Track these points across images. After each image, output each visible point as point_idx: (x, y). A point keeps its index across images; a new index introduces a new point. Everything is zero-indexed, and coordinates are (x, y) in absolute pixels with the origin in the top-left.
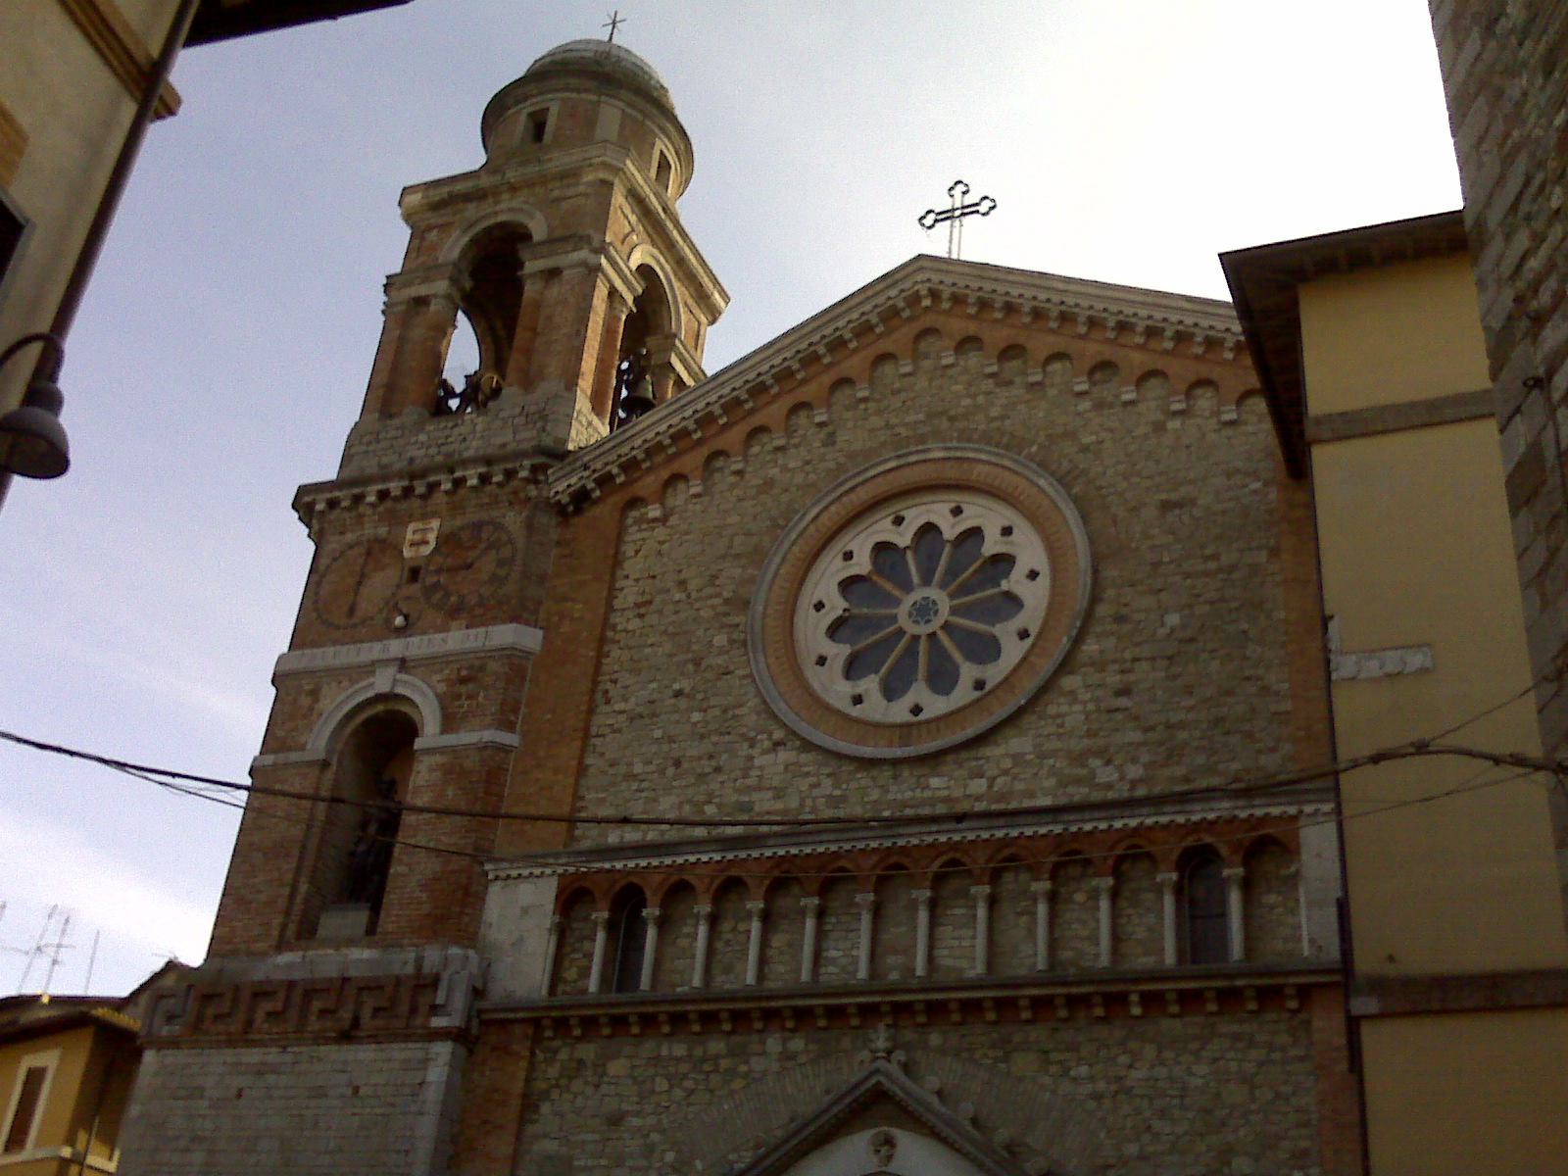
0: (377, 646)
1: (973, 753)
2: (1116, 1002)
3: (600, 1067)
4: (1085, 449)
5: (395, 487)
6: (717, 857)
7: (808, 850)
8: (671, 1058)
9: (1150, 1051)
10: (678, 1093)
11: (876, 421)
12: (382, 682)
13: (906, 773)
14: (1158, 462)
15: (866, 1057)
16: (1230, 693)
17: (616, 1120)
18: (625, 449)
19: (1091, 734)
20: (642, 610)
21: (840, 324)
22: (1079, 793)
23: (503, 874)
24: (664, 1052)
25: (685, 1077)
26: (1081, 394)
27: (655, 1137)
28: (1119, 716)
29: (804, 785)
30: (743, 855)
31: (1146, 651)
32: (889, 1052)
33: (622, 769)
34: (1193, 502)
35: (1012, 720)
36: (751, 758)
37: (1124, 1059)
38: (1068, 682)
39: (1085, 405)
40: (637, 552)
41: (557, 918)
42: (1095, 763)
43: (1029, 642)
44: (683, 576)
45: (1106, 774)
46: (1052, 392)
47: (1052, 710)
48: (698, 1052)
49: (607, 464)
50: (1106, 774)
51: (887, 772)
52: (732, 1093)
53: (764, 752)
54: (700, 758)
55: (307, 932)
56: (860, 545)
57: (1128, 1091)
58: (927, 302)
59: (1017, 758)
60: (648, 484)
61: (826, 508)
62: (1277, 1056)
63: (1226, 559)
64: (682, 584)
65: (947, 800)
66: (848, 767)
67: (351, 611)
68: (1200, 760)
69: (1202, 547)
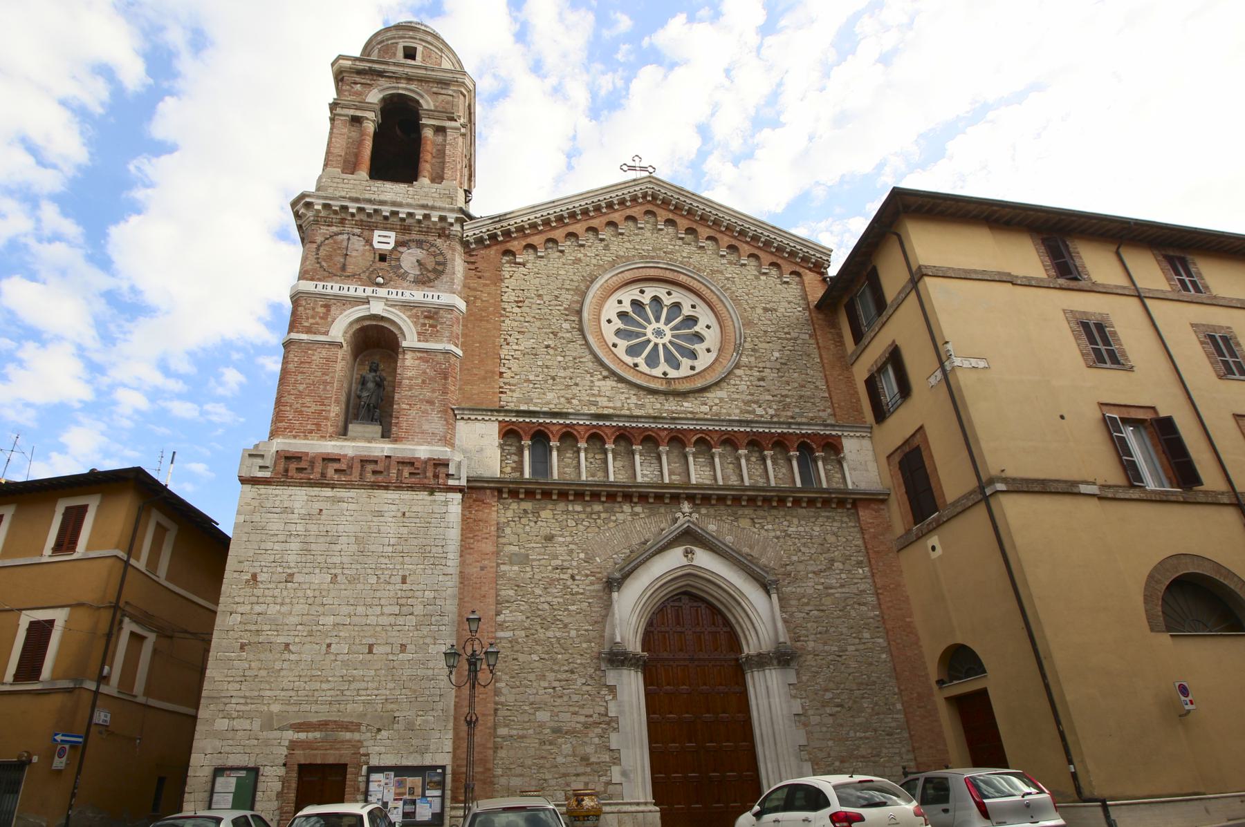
2: (782, 501)
3: (536, 513)
9: (795, 521)
11: (628, 245)
17: (550, 538)
22: (750, 417)
24: (570, 508)
35: (717, 384)
42: (755, 406)
48: (589, 509)
51: (661, 399)
59: (721, 399)
64: (540, 296)
65: (691, 413)
66: (642, 393)
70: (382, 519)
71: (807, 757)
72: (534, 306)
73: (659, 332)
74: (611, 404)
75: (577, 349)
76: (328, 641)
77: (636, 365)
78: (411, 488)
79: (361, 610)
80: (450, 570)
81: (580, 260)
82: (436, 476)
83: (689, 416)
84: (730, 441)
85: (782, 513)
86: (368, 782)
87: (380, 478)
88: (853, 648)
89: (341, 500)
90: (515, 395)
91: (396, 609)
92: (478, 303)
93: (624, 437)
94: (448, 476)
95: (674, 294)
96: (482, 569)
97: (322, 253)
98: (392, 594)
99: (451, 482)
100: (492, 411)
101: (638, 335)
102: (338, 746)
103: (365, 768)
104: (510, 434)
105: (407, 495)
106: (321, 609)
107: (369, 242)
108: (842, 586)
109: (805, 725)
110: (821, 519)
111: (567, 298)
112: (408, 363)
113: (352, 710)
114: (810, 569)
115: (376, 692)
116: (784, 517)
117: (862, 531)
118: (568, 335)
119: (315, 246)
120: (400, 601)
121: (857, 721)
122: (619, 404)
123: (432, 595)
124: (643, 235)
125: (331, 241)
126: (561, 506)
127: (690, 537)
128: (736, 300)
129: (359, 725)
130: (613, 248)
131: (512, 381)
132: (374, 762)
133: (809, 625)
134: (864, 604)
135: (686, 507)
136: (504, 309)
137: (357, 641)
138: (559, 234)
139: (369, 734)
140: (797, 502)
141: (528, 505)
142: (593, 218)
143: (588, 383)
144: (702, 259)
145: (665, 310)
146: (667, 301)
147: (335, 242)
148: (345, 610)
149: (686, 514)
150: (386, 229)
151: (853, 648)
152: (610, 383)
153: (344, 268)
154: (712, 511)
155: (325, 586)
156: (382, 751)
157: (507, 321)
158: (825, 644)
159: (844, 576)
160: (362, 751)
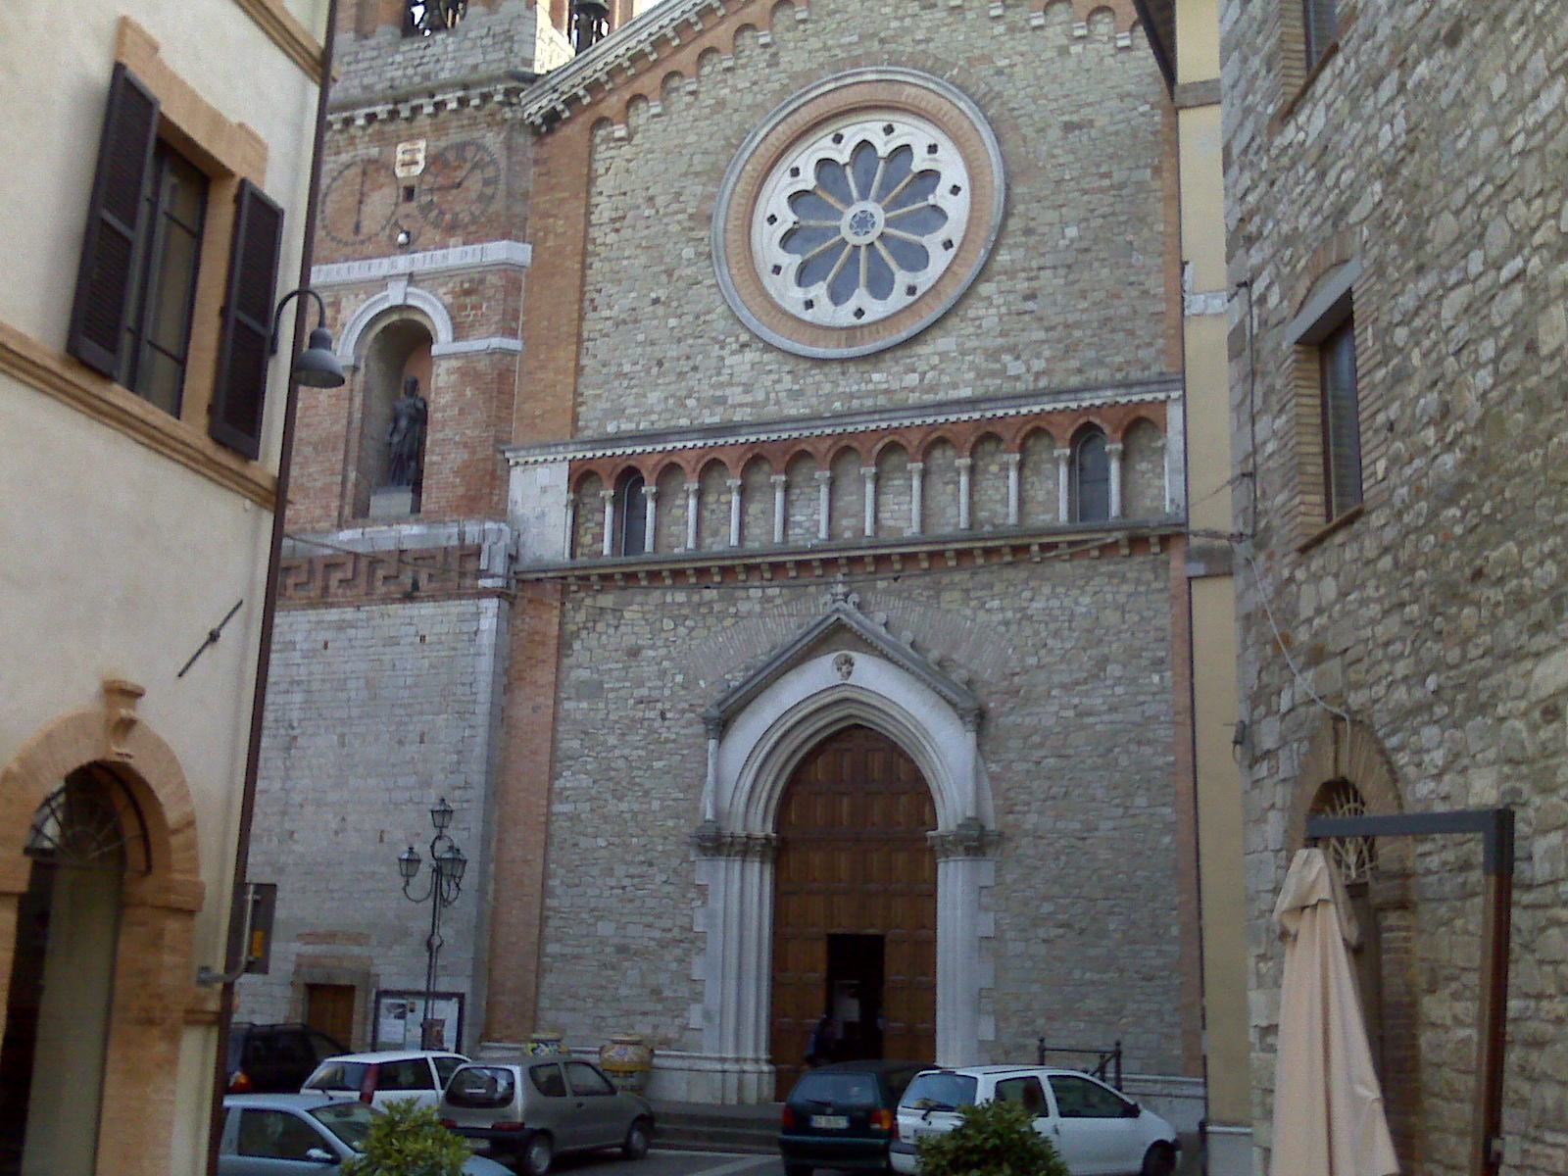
0: (386, 262)
1: (907, 352)
3: (617, 611)
4: (1000, 72)
5: (381, 110)
6: (700, 444)
7: (774, 437)
10: (682, 631)
12: (395, 295)
13: (852, 369)
14: (1062, 84)
15: (826, 601)
16: (1117, 296)
17: (634, 653)
18: (588, 72)
19: (1003, 334)
20: (617, 225)
22: (992, 384)
23: (522, 461)
24: (669, 599)
25: (686, 618)
27: (666, 664)
28: (1027, 318)
29: (768, 380)
30: (721, 442)
31: (1048, 260)
32: (846, 596)
33: (614, 369)
34: (1091, 123)
36: (722, 359)
38: (985, 289)
39: (1000, 29)
40: (607, 170)
41: (572, 496)
42: (1007, 358)
43: (952, 251)
44: (651, 192)
45: (1015, 368)
46: (970, 15)
47: (971, 313)
48: (696, 598)
49: (573, 86)
50: (1015, 368)
51: (837, 369)
53: (733, 353)
54: (678, 359)
55: (361, 512)
56: (805, 161)
59: (943, 355)
60: (612, 104)
61: (774, 128)
62: (1142, 589)
63: (1117, 177)
65: (886, 391)
66: (803, 365)
67: (357, 229)
69: (1098, 165)
74: (748, 399)
83: (882, 401)
85: (1023, 575)
110: (1097, 581)
122: (761, 396)
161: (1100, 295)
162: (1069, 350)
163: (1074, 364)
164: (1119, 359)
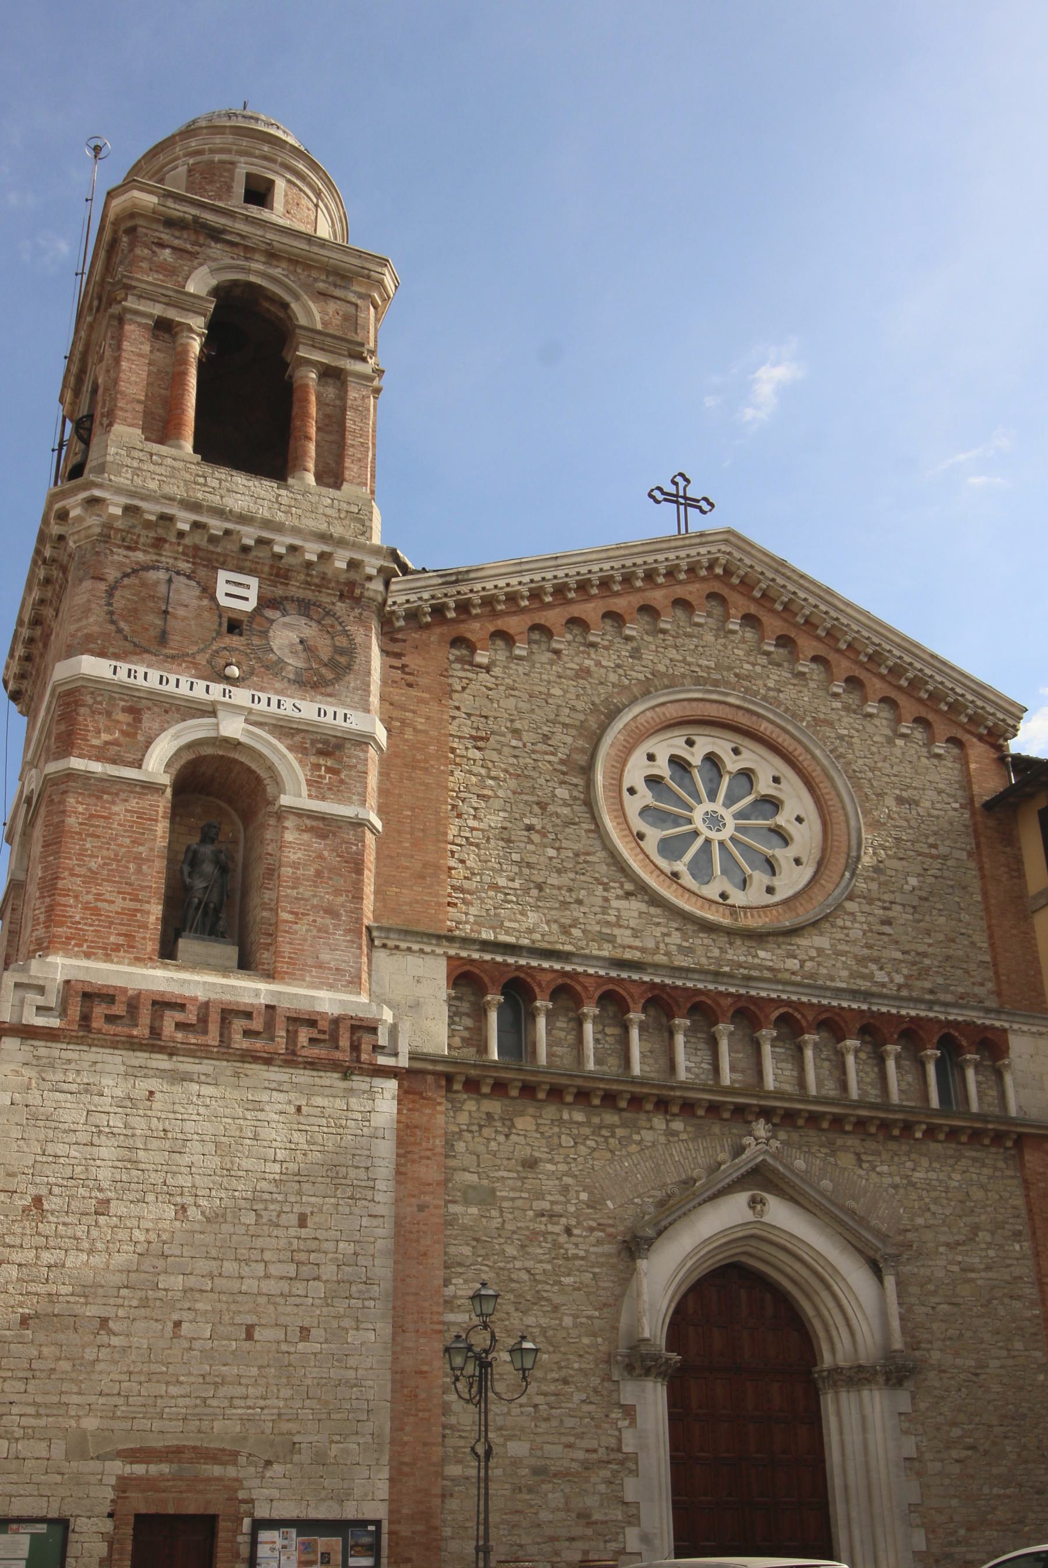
1: (788, 940)
3: (508, 1121)
4: (841, 738)
7: (679, 983)
8: (571, 1121)
9: (925, 1162)
10: (582, 1149)
11: (672, 653)
13: (739, 942)
20: (480, 744)
21: (639, 561)
22: (864, 985)
25: (587, 1138)
26: (836, 695)
27: (567, 1180)
28: (885, 938)
30: (624, 975)
35: (815, 924)
37: (909, 1164)
39: (837, 705)
40: (464, 688)
42: (873, 967)
47: (840, 922)
48: (596, 1120)
51: (722, 940)
52: (629, 1155)
53: (618, 897)
54: (559, 888)
57: (914, 1185)
58: (719, 571)
59: (820, 951)
62: (998, 1174)
63: (943, 850)
64: (516, 733)
65: (770, 969)
68: (940, 980)
70: (261, 1115)
71: (919, 1521)
72: (506, 750)
73: (717, 820)
74: (637, 943)
75: (578, 839)
76: (175, 1317)
77: (675, 875)
78: (312, 1065)
79: (230, 1267)
80: (380, 1210)
81: (588, 672)
82: (355, 1048)
83: (767, 974)
84: (832, 1025)
85: (905, 1148)
86: (254, 1543)
87: (259, 1044)
88: (997, 1363)
89: (186, 1078)
90: (473, 910)
91: (291, 1270)
92: (409, 735)
93: (662, 1003)
94: (376, 1048)
95: (745, 754)
96: (421, 1208)
97: (119, 602)
98: (283, 1243)
99: (382, 1060)
100: (439, 937)
101: (676, 820)
102: (201, 1487)
103: (247, 1522)
104: (465, 980)
105: (303, 1077)
106: (160, 1263)
107: (208, 591)
108: (988, 1268)
109: (919, 1474)
110: (964, 1162)
111: (565, 740)
112: (289, 836)
113: (223, 1430)
114: (942, 1239)
115: (262, 1403)
116: (908, 1154)
117: (1026, 1184)
118: (566, 811)
119: (103, 586)
120: (297, 1256)
121: (995, 1471)
122: (650, 944)
123: (350, 1248)
124: (700, 637)
125: (132, 580)
126: (550, 1111)
127: (761, 1179)
128: (853, 777)
129: (236, 1454)
130: (648, 656)
131: (467, 884)
132: (262, 1512)
133: (935, 1326)
134: (1019, 1298)
135: (761, 1128)
136: (453, 750)
137: (226, 1318)
138: (554, 618)
139: (252, 1470)
140: (931, 1132)
141: (495, 1106)
142: (617, 594)
143: (599, 901)
144: (797, 695)
145: (726, 780)
146: (732, 764)
147: (143, 584)
148: (203, 1266)
149: (760, 1141)
150: (240, 570)
151: (997, 1363)
152: (636, 905)
153: (163, 638)
154: (795, 1136)
155: (166, 1225)
156: (274, 1495)
157: (457, 773)
158: (956, 1354)
159: (991, 1253)
160: (241, 1495)
161: (941, 937)
162: (924, 973)
163: (928, 985)
164: (961, 990)
